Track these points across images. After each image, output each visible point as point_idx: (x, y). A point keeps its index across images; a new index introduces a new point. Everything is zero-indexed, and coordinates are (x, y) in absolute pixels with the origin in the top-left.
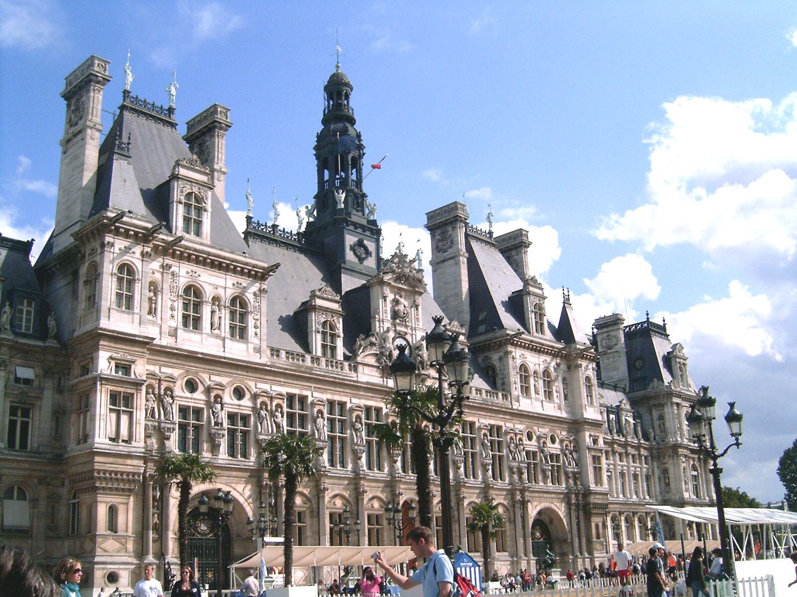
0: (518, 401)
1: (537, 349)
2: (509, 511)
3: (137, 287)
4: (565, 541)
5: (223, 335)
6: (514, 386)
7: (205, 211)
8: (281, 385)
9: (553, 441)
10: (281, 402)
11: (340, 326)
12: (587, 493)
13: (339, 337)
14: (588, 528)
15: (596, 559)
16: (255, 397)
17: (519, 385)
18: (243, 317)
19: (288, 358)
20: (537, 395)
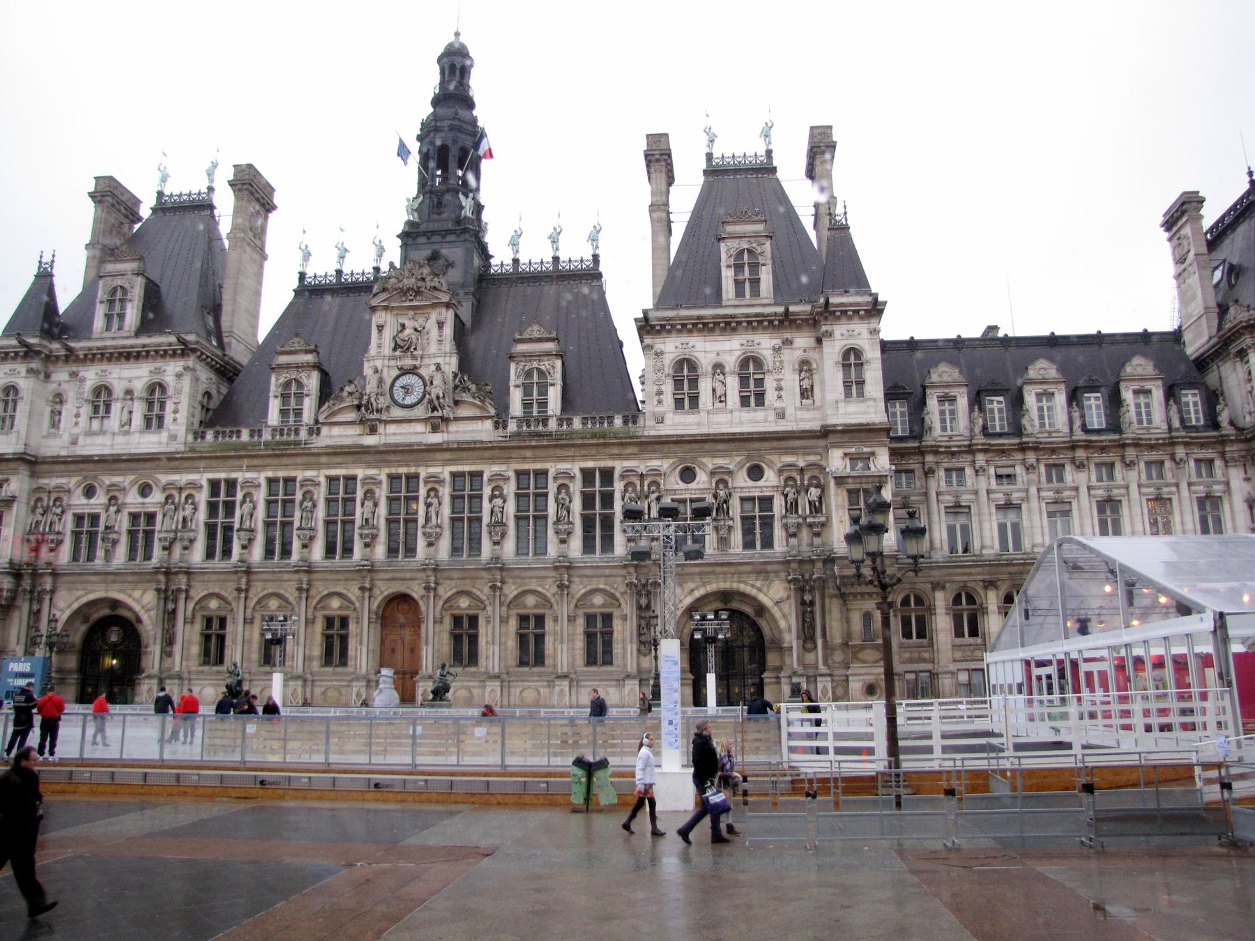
0: (660, 420)
1: (728, 326)
2: (617, 600)
3: (20, 406)
4: (779, 647)
5: (132, 430)
6: (657, 397)
7: (130, 301)
8: (199, 472)
9: (756, 473)
10: (193, 492)
11: (312, 382)
12: (830, 560)
13: (307, 395)
14: (848, 621)
15: (850, 678)
16: (164, 489)
17: (668, 399)
18: (162, 406)
19: (216, 437)
20: (718, 405)
